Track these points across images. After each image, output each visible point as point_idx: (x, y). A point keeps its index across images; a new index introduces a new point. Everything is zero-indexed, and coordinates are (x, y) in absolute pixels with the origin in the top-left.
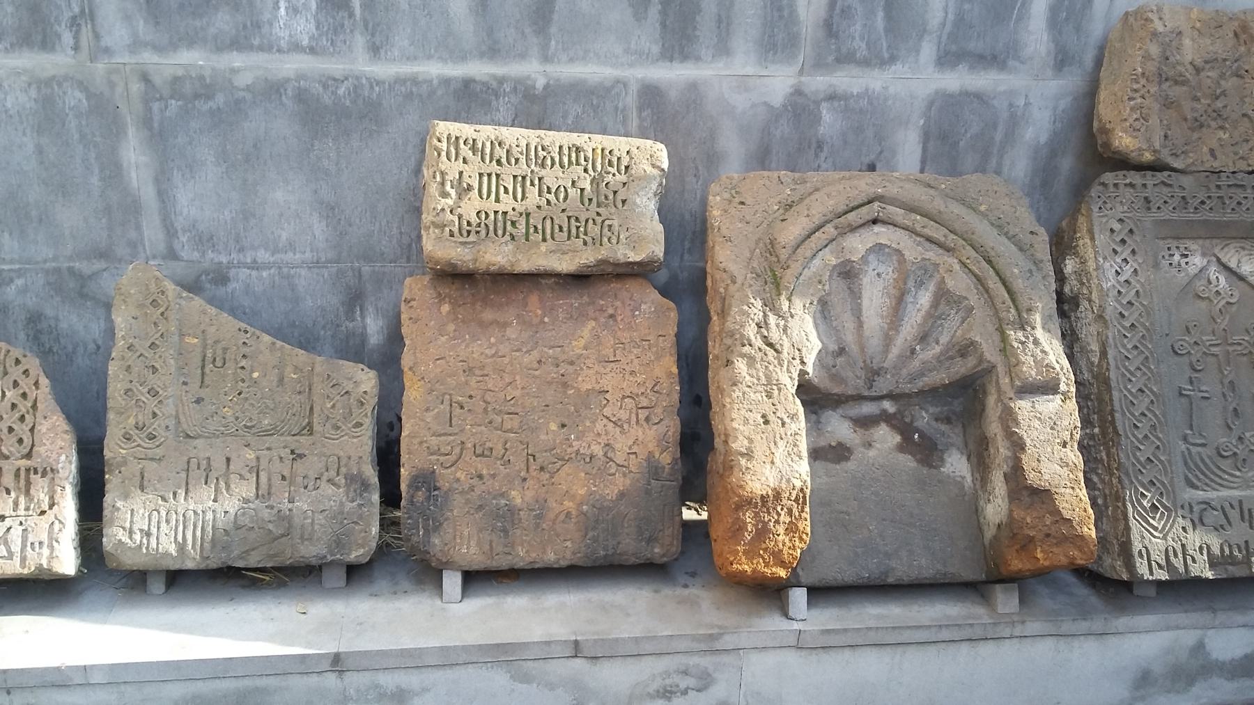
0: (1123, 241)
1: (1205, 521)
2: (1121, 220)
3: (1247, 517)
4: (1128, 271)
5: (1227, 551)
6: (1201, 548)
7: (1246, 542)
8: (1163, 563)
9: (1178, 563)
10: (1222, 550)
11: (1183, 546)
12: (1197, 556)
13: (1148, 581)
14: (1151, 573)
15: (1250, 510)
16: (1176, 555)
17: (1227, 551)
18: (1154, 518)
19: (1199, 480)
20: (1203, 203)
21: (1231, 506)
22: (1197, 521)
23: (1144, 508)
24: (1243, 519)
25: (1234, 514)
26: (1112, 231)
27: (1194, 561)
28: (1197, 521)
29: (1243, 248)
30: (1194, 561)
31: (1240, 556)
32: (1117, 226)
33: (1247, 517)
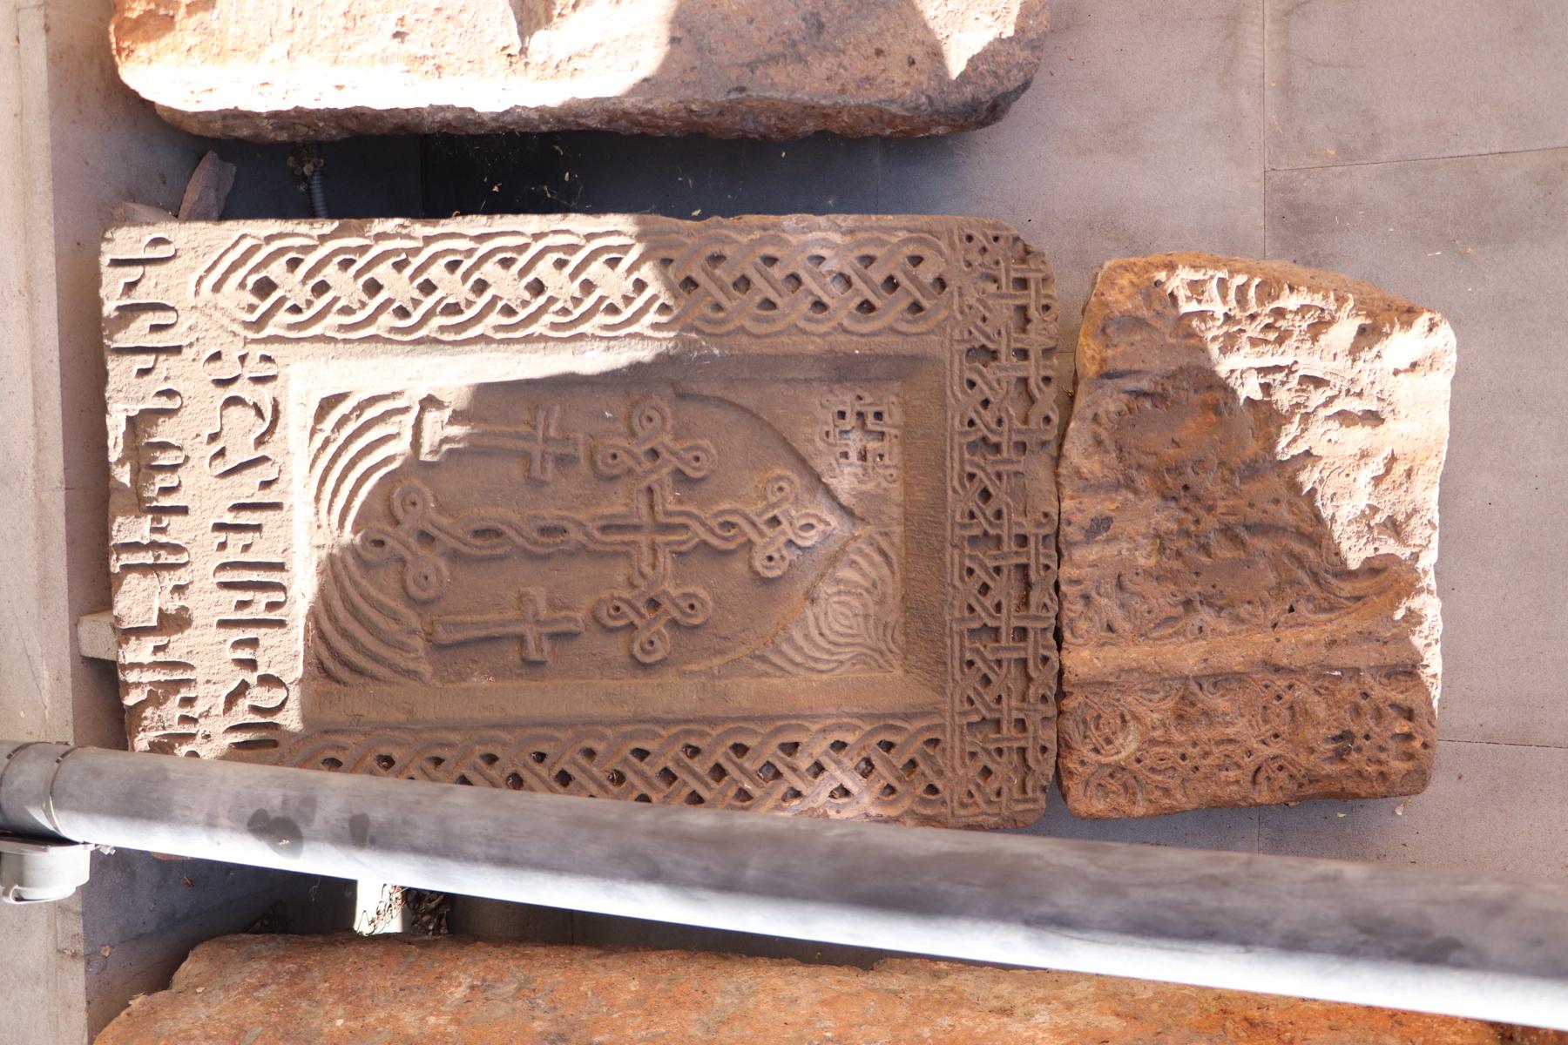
0: (891, 284)
1: (234, 412)
2: (941, 283)
3: (246, 518)
4: (832, 294)
5: (165, 459)
6: (170, 393)
7: (183, 511)
8: (139, 297)
9: (137, 333)
10: (165, 446)
11: (177, 350)
12: (155, 383)
13: (98, 253)
14: (116, 263)
15: (258, 528)
16: (156, 328)
17: (165, 459)
18: (242, 285)
19: (339, 425)
20: (986, 495)
21: (266, 485)
22: (233, 391)
23: (265, 263)
24: (239, 507)
25: (246, 487)
26: (916, 260)
27: (143, 372)
28: (233, 391)
29: (881, 602)
30: (143, 372)
31: (152, 491)
32: (927, 274)
33: (246, 518)
